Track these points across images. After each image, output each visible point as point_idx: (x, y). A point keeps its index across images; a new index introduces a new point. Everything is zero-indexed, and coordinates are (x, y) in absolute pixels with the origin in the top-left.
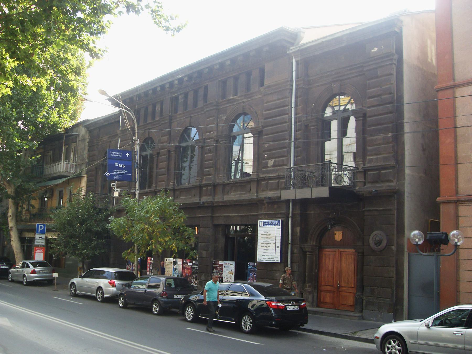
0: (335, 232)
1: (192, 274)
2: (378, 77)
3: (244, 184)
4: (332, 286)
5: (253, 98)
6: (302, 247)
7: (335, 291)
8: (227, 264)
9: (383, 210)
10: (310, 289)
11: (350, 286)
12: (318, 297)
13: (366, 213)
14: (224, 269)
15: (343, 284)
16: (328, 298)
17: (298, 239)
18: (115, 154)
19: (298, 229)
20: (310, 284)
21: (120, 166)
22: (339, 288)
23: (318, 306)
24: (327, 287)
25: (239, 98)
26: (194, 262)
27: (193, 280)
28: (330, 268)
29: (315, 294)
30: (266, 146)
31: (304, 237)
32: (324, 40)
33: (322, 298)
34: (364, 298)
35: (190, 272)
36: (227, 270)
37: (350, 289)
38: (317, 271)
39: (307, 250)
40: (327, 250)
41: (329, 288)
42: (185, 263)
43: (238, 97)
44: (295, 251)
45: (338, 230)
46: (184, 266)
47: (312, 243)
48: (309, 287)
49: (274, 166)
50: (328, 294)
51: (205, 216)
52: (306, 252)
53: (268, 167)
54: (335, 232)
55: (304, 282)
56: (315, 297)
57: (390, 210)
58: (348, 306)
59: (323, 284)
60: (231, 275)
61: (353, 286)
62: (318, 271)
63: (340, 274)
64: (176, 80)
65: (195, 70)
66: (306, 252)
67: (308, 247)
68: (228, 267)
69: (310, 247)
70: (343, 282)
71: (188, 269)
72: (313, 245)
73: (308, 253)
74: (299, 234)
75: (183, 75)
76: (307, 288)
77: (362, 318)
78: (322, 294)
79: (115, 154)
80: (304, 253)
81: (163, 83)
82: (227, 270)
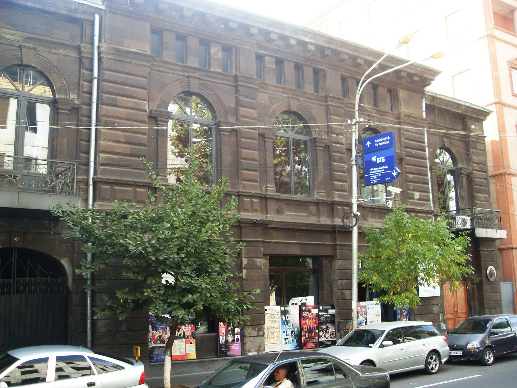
1: (320, 324)
2: (476, 149)
3: (384, 211)
5: (385, 117)
8: (371, 304)
9: (491, 251)
13: (481, 252)
14: (368, 311)
15: (459, 311)
18: (381, 142)
21: (378, 162)
25: (370, 110)
26: (321, 308)
27: (321, 333)
30: (411, 176)
32: (453, 100)
35: (315, 323)
36: (372, 312)
42: (305, 311)
43: (370, 108)
46: (304, 314)
49: (419, 199)
51: (345, 245)
53: (413, 198)
57: (493, 251)
60: (378, 317)
64: (295, 39)
65: (333, 47)
68: (373, 308)
71: (310, 319)
75: (313, 41)
79: (381, 142)
81: (271, 29)
82: (372, 312)
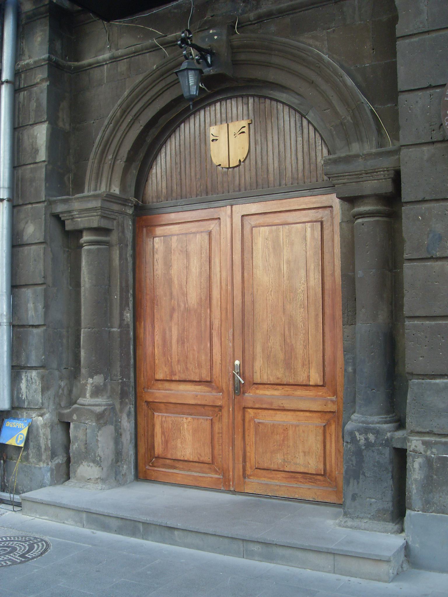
0: (213, 130)
4: (208, 383)
6: (60, 208)
7: (220, 408)
10: (98, 403)
11: (301, 378)
12: (142, 436)
15: (261, 371)
16: (186, 438)
17: (42, 174)
19: (41, 134)
20: (98, 379)
22: (239, 390)
23: (141, 476)
24: (182, 387)
28: (193, 297)
29: (127, 424)
31: (67, 168)
33: (158, 440)
34: (415, 444)
37: (300, 392)
38: (128, 316)
39: (82, 222)
40: (173, 217)
41: (188, 393)
44: (31, 231)
45: (227, 120)
47: (105, 183)
48: (97, 392)
50: (187, 423)
52: (79, 233)
54: (213, 130)
55: (74, 373)
56: (127, 438)
58: (293, 475)
59: (160, 375)
61: (315, 378)
62: (137, 317)
63: (243, 322)
66: (79, 233)
67: (83, 209)
69: (97, 204)
70: (259, 364)
72: (110, 198)
73: (86, 237)
74: (42, 155)
76: (87, 400)
77: (410, 559)
78: (159, 418)
80: (73, 236)
